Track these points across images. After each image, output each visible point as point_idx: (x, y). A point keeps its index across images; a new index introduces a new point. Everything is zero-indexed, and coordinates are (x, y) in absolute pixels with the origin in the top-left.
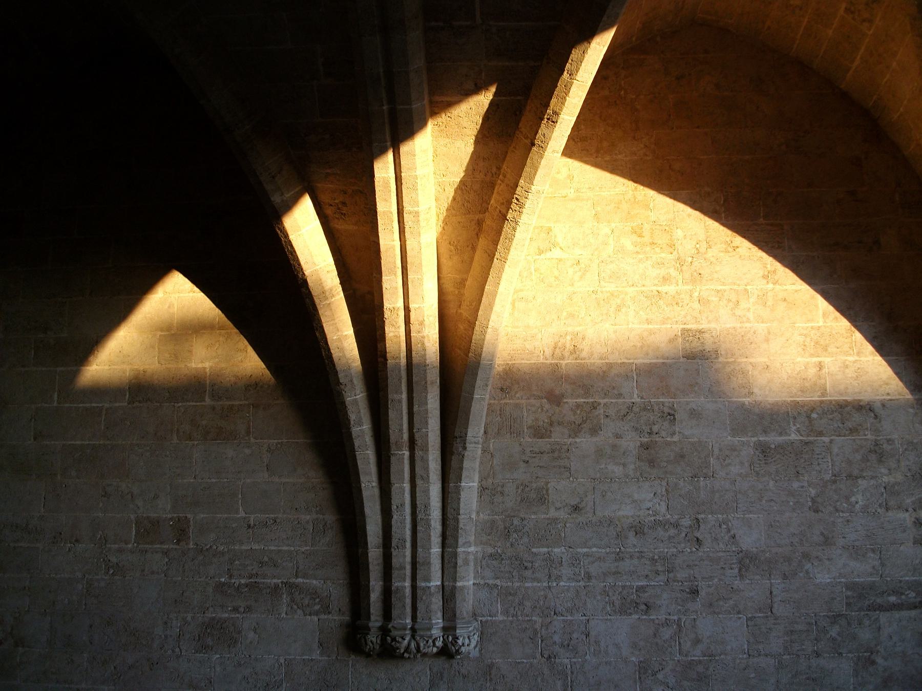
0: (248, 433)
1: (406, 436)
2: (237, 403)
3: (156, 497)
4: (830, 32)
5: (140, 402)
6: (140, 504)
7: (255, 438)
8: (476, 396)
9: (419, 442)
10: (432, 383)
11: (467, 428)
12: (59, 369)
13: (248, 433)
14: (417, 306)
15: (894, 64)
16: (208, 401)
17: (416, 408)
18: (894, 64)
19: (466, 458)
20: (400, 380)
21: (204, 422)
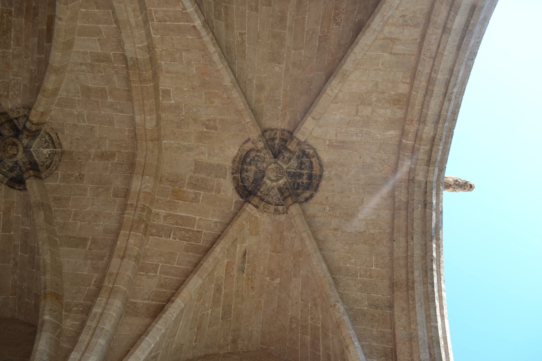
4: (309, 338)
15: (331, 334)
18: (331, 334)
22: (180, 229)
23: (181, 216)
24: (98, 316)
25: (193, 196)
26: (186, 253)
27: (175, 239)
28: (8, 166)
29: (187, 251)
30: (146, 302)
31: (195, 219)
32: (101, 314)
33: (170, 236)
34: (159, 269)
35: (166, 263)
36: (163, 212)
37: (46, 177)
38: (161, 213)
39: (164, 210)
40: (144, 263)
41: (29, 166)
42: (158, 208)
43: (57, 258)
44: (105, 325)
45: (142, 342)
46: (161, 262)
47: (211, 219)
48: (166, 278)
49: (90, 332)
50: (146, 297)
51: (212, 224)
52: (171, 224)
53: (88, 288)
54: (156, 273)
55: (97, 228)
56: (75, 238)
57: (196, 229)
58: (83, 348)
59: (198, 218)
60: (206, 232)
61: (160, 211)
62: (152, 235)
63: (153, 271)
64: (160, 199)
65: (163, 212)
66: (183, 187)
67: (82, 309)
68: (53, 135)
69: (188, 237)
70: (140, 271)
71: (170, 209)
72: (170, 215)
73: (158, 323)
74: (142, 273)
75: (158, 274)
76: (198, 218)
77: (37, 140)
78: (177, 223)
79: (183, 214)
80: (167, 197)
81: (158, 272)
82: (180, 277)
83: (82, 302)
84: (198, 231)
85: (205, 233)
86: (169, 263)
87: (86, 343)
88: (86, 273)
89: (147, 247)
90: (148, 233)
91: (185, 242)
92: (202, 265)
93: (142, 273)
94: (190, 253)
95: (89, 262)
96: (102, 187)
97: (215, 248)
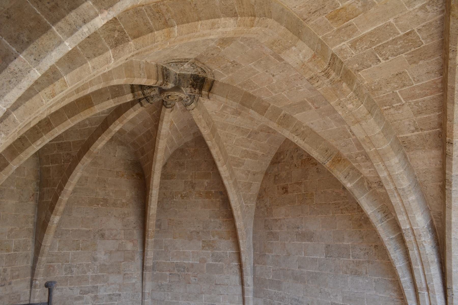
0: (367, 273)
1: (424, 285)
2: (361, 260)
3: (336, 296)
5: (329, 257)
6: (332, 297)
7: (369, 276)
8: (453, 270)
9: (430, 289)
10: (432, 262)
11: (452, 285)
12: (303, 243)
13: (367, 273)
14: (416, 228)
16: (351, 258)
17: (426, 273)
19: (454, 299)
20: (416, 259)
21: (351, 267)
22: (383, 46)
23: (371, 33)
24: (388, 179)
25: (360, 4)
26: (414, 65)
27: (388, 59)
28: (187, 98)
29: (415, 62)
30: (416, 133)
31: (390, 25)
32: (389, 175)
33: (379, 60)
34: (400, 96)
35: (402, 87)
36: (345, 44)
37: (214, 76)
38: (344, 47)
39: (344, 41)
40: (379, 98)
41: (197, 91)
42: (334, 45)
43: (302, 129)
44: (402, 185)
45: (451, 194)
46: (395, 88)
47: (411, 9)
48: (417, 102)
49: (396, 194)
50: (412, 128)
51: (419, 13)
52: (367, 48)
53: (350, 138)
54: (401, 101)
55: (300, 90)
56: (295, 105)
57: (402, 33)
58: (402, 209)
59: (391, 20)
60: (419, 27)
61: (341, 45)
62: (358, 71)
63: (395, 101)
64: (326, 36)
65: (345, 44)
66: (337, 5)
67: (364, 157)
68: (173, 61)
69: (401, 48)
70: (382, 107)
71: (349, 36)
72: (356, 41)
73: (453, 171)
74: (385, 108)
75: (404, 102)
76: (391, 20)
77: (170, 68)
78: (372, 43)
79: (369, 30)
80: (332, 28)
81: (402, 99)
82: (431, 94)
83: (358, 151)
84: (407, 34)
85: (419, 30)
86: (404, 85)
87: (400, 204)
88: (335, 127)
89: (366, 83)
90: (353, 72)
91: (403, 55)
92: (453, 89)
93: (385, 108)
94: (421, 62)
95: (328, 118)
96: (262, 60)
97: (455, 59)
